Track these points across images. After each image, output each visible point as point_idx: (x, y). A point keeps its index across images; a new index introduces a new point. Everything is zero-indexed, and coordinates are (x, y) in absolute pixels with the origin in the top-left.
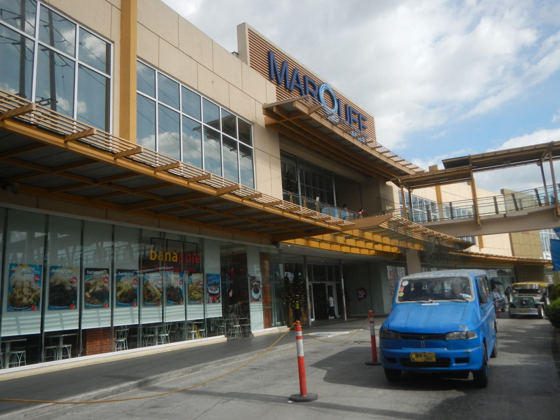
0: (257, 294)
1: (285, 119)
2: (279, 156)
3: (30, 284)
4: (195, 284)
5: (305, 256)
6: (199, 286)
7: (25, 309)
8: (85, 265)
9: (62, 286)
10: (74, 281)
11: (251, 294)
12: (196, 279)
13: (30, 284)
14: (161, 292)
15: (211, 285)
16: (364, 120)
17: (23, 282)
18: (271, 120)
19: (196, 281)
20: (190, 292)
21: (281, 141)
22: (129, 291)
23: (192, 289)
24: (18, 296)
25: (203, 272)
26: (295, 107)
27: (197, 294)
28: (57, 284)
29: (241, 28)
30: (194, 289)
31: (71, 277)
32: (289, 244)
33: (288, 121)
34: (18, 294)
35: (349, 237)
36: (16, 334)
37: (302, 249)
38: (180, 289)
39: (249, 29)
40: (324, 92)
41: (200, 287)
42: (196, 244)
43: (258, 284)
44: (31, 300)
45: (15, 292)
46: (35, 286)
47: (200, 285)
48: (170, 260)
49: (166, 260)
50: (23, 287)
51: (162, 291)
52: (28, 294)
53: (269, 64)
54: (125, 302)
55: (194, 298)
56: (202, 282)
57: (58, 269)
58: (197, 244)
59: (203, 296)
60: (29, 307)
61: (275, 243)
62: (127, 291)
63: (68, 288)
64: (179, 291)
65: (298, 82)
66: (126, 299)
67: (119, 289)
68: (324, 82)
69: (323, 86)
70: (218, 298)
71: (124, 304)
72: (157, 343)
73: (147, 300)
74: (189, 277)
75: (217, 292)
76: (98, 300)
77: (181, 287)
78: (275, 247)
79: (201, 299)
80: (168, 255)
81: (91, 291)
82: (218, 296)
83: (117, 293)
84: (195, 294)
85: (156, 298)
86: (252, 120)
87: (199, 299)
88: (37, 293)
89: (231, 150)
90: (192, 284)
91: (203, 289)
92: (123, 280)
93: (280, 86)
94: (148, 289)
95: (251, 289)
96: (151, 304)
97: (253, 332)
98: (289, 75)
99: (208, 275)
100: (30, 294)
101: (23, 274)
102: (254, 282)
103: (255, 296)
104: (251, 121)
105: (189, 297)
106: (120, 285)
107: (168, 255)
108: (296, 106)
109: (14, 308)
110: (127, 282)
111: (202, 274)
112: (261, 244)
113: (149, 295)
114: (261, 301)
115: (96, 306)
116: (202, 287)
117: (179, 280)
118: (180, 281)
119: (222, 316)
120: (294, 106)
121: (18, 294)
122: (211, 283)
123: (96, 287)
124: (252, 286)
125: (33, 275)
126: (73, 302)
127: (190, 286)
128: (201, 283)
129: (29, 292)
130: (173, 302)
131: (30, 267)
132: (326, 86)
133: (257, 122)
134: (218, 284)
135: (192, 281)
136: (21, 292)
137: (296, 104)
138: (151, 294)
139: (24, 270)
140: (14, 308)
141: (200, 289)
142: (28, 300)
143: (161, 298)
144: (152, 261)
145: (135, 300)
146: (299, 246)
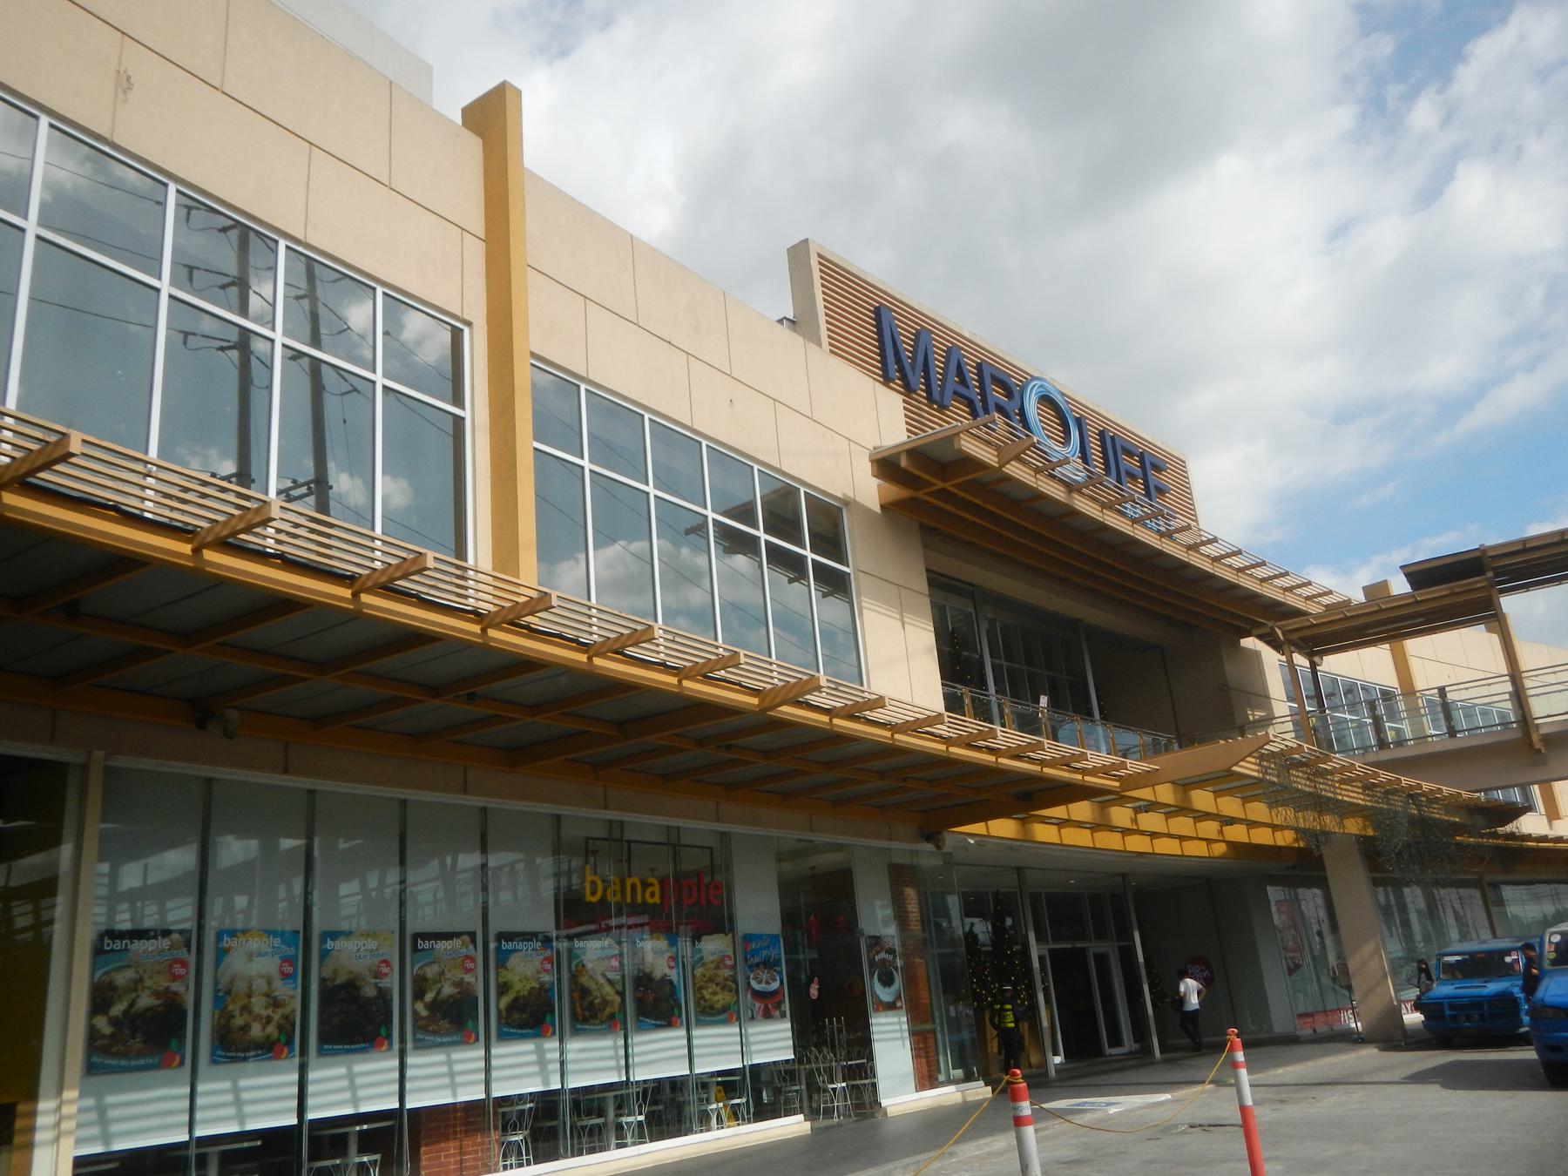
0: (889, 986)
1: (934, 485)
2: (924, 588)
3: (269, 983)
4: (712, 966)
5: (1019, 870)
6: (723, 971)
7: (257, 1055)
8: (411, 928)
9: (352, 986)
10: (385, 970)
11: (872, 987)
12: (714, 950)
13: (269, 983)
14: (618, 993)
15: (758, 965)
17: (250, 981)
18: (896, 492)
19: (711, 958)
20: (699, 989)
21: (925, 546)
22: (530, 994)
23: (705, 979)
24: (239, 1021)
25: (732, 930)
26: (960, 450)
28: (338, 981)
29: (798, 254)
30: (711, 980)
31: (376, 960)
32: (972, 835)
33: (943, 490)
34: (237, 1013)
35: (1145, 806)
36: (233, 1128)
37: (1010, 848)
38: (671, 982)
39: (819, 256)
40: (1038, 403)
41: (727, 973)
42: (708, 851)
43: (891, 957)
44: (271, 1029)
45: (231, 1008)
46: (282, 989)
47: (726, 967)
48: (639, 900)
49: (629, 900)
50: (249, 996)
51: (620, 989)
52: (264, 1013)
53: (881, 340)
54: (521, 1027)
55: (712, 1007)
56: (730, 959)
57: (343, 937)
58: (711, 848)
59: (735, 999)
60: (270, 1049)
61: (931, 835)
62: (526, 993)
64: (667, 989)
65: (963, 381)
66: (524, 1016)
67: (503, 988)
68: (1036, 374)
70: (778, 1005)
71: (519, 1031)
72: (614, 1142)
73: (581, 1019)
74: (694, 945)
75: (775, 985)
76: (449, 1023)
77: (674, 975)
78: (930, 847)
79: (730, 1008)
80: (633, 886)
81: (429, 997)
82: (777, 1000)
83: (498, 1001)
84: (715, 993)
85: (604, 1009)
86: (844, 495)
87: (725, 1009)
88: (286, 1010)
89: (791, 581)
90: (704, 964)
91: (735, 981)
92: (514, 961)
93: (915, 396)
94: (582, 985)
96: (592, 1027)
97: (884, 1102)
98: (937, 364)
99: (748, 938)
100: (269, 1012)
101: (250, 956)
102: (878, 953)
103: (885, 994)
104: (841, 496)
105: (697, 1004)
106: (507, 976)
107: (633, 886)
108: (963, 448)
109: (228, 1054)
110: (526, 968)
111: (730, 935)
112: (891, 839)
113: (586, 1004)
114: (901, 1007)
115: (444, 1040)
116: (731, 973)
117: (667, 955)
118: (669, 958)
119: (793, 1057)
120: (956, 447)
121: (237, 1013)
122: (757, 960)
123: (442, 986)
124: (872, 963)
125: (277, 960)
126: (383, 1031)
127: (699, 971)
128: (729, 963)
129: (266, 1008)
130: (653, 1022)
131: (269, 937)
132: (1041, 386)
133: (857, 499)
134: (777, 962)
135: (702, 958)
136: (246, 1009)
137: (962, 442)
138: (593, 1001)
139: (254, 944)
140: (228, 1054)
141: (726, 979)
142: (264, 1029)
143: (620, 1011)
144: (590, 903)
145: (548, 1019)
146: (1001, 841)
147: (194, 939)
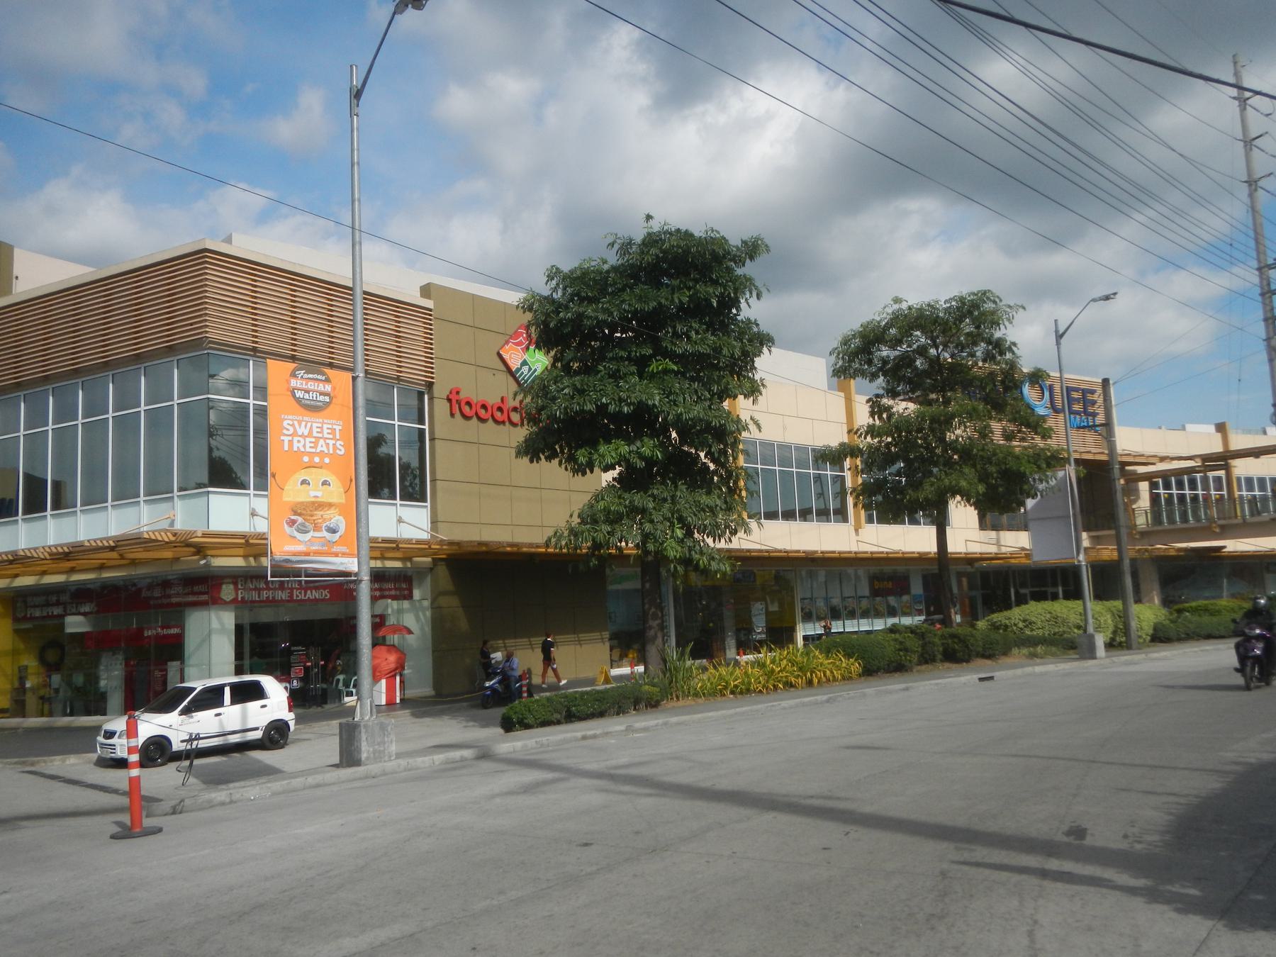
8: (844, 596)
63: (837, 609)
67: (860, 608)
70: (922, 612)
75: (921, 608)
77: (896, 605)
99: (914, 596)
147: (811, 599)
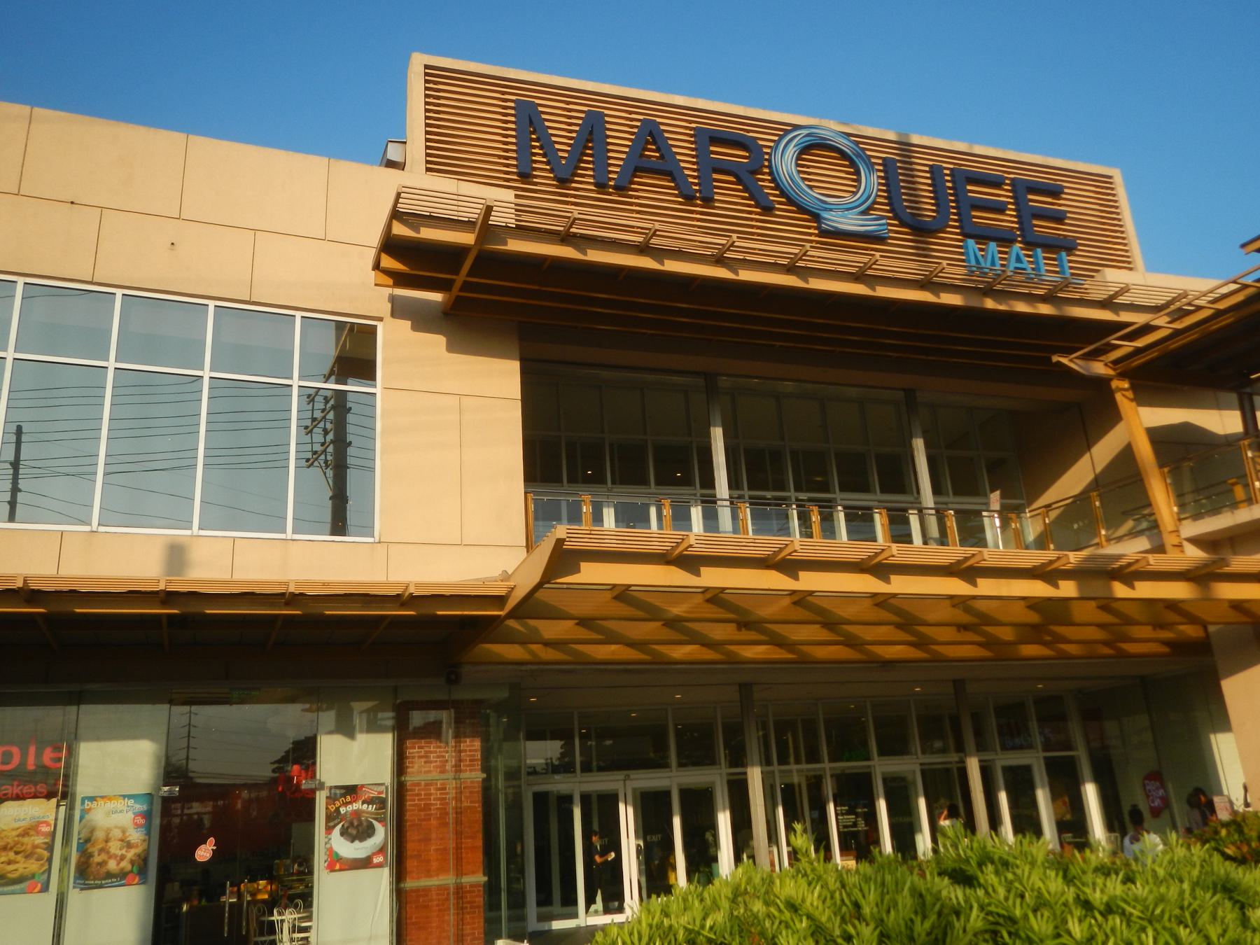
4: (14, 833)
16: (1055, 192)
27: (18, 863)
41: (39, 840)
43: (372, 808)
47: (38, 833)
59: (46, 867)
69: (799, 134)
84: (9, 863)
91: (50, 848)
93: (574, 185)
95: (329, 829)
98: (620, 143)
114: (380, 865)
116: (46, 840)
124: (332, 818)
128: (45, 829)
141: (36, 847)
